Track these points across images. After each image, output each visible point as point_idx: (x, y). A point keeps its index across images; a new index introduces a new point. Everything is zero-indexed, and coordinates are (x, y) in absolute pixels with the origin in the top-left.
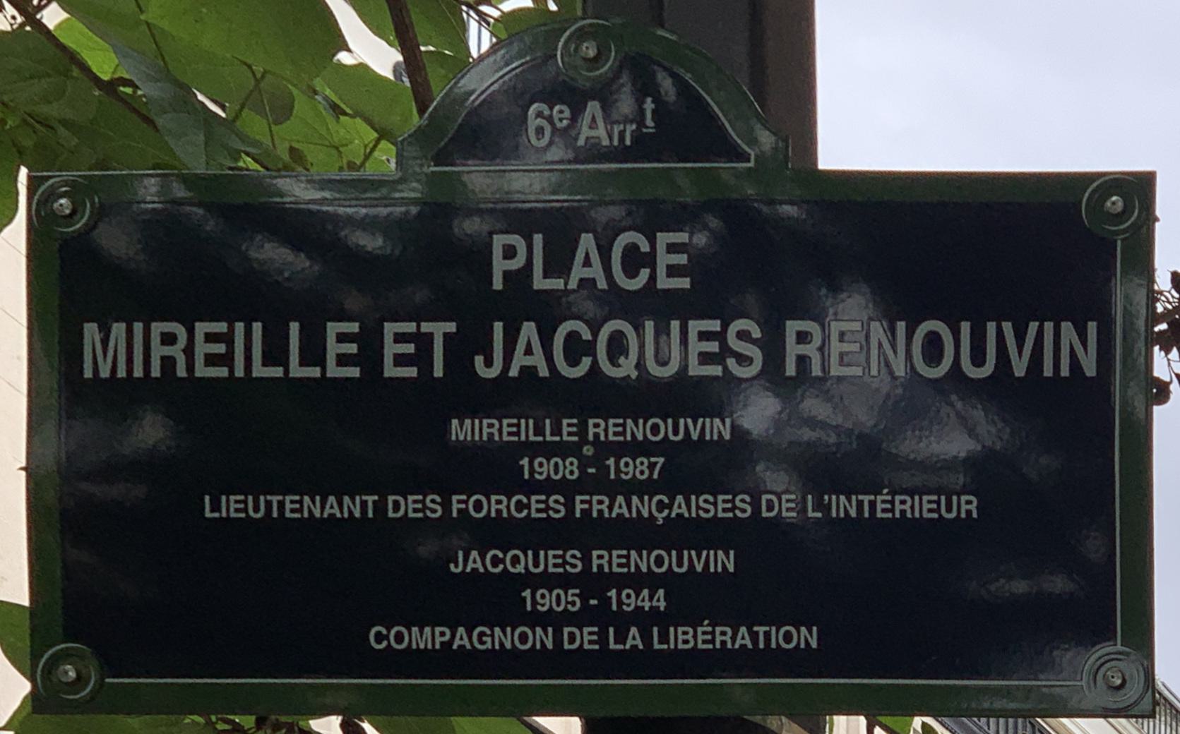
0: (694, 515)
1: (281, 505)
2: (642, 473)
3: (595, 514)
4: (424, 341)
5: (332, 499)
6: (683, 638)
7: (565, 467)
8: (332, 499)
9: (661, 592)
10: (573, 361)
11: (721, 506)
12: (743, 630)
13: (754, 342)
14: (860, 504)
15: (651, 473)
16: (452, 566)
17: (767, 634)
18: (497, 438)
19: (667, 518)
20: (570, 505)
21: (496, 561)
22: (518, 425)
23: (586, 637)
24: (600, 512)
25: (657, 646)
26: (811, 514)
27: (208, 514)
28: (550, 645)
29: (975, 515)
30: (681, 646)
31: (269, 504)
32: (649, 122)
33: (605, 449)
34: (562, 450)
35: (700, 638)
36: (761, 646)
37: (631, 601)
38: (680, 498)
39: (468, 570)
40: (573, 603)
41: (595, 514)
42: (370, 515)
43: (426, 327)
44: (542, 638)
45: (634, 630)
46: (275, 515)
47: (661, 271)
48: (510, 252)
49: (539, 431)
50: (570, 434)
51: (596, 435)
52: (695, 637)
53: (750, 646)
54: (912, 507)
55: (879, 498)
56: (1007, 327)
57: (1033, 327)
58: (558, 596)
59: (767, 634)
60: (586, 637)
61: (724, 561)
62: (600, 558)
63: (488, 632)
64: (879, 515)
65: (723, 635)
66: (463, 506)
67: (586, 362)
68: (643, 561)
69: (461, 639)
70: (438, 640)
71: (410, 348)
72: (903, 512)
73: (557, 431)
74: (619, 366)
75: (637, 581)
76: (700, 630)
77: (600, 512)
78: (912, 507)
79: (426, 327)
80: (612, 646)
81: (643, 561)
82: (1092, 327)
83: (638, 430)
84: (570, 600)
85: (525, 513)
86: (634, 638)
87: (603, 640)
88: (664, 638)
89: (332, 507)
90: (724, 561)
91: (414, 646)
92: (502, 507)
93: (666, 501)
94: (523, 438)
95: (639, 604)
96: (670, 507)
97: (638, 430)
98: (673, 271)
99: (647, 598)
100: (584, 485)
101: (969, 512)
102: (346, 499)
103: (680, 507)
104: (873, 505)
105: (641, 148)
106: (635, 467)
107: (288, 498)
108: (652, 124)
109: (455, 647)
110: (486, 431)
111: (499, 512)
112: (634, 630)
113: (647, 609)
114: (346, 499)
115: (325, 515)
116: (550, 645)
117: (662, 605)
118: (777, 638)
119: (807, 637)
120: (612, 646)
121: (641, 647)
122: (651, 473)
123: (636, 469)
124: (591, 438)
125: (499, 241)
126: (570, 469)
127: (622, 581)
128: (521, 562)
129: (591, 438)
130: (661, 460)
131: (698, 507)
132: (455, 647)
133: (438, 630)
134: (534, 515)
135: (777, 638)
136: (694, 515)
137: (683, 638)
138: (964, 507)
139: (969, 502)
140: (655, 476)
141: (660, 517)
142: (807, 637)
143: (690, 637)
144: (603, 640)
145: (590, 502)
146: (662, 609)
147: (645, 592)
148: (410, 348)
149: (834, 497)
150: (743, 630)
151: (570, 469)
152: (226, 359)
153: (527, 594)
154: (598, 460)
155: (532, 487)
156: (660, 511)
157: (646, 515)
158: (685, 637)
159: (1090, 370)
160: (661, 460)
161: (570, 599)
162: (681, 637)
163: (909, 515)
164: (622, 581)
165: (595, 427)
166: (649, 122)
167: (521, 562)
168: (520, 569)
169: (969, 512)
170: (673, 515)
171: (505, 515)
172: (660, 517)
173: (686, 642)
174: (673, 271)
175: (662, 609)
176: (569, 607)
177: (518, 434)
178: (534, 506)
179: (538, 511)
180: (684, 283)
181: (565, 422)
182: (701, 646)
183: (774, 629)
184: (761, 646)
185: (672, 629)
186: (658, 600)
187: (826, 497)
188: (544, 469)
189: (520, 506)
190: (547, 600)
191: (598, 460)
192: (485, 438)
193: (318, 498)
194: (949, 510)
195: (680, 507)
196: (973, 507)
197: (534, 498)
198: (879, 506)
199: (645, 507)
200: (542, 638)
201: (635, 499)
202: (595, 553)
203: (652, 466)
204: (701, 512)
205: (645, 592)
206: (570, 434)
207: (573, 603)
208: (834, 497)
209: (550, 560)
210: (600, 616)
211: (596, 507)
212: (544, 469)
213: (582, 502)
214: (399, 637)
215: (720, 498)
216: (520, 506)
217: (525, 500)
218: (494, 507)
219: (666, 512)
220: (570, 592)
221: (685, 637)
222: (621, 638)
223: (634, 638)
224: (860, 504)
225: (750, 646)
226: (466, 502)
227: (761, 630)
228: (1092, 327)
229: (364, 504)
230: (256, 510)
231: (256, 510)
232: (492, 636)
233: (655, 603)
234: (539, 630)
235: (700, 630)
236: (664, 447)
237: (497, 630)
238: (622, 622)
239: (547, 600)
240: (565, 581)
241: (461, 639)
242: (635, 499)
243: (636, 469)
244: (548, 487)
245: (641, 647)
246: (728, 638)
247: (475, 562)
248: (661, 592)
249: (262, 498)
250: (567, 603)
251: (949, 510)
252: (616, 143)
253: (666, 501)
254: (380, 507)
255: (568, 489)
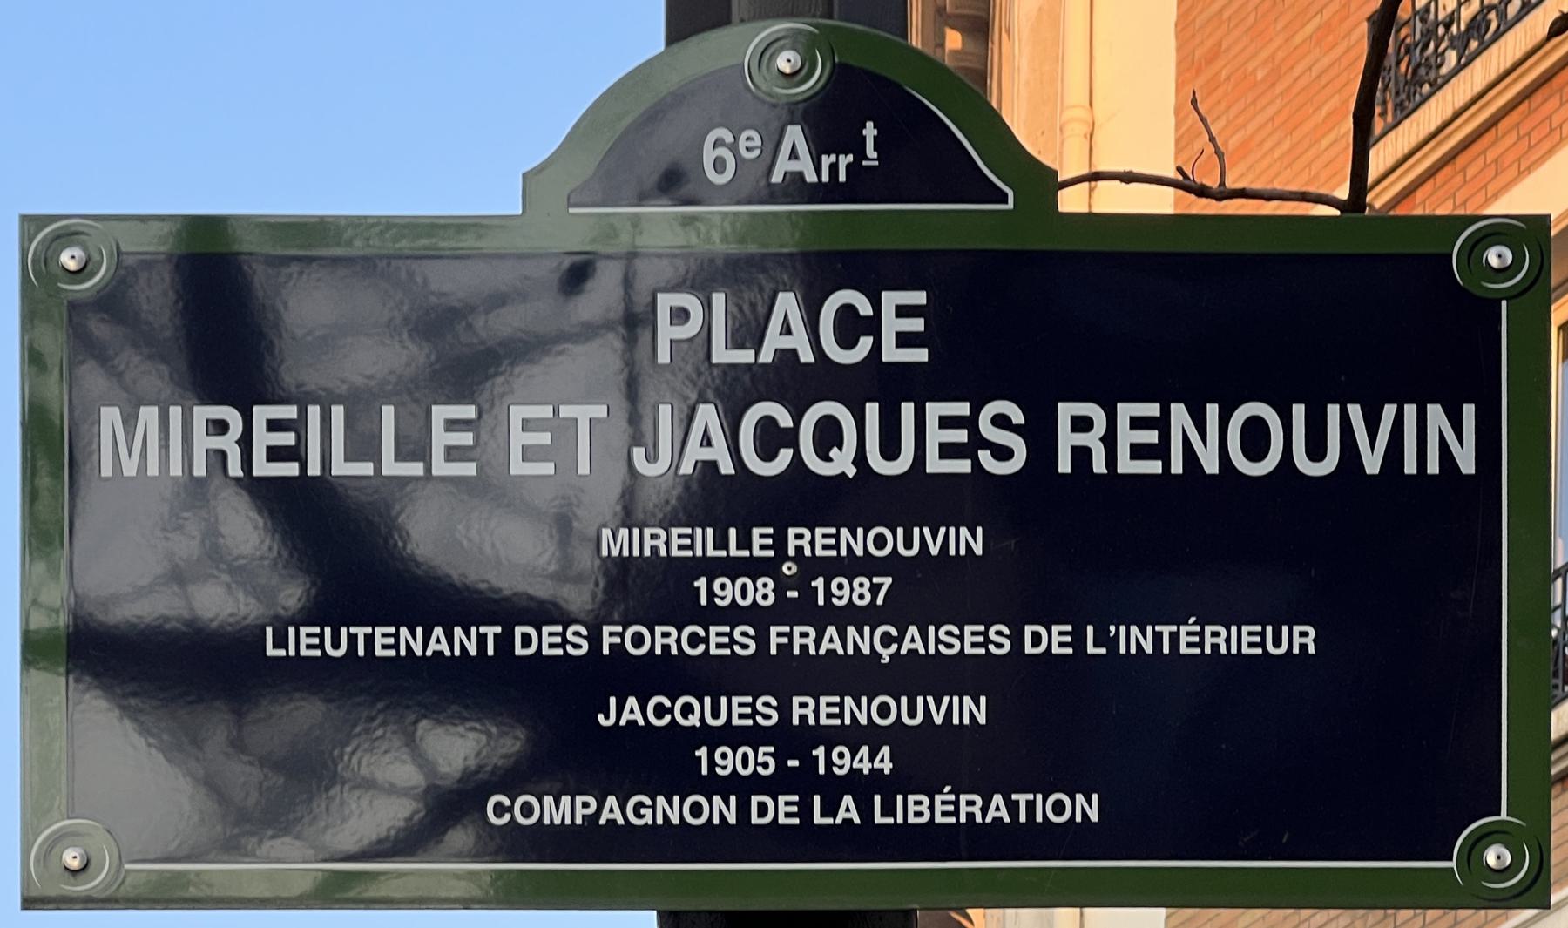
0: (932, 651)
1: (370, 639)
2: (861, 597)
3: (796, 651)
4: (563, 431)
5: (438, 631)
6: (914, 809)
7: (756, 590)
8: (438, 631)
9: (886, 750)
10: (767, 455)
11: (968, 639)
12: (998, 799)
13: (1016, 429)
14: (1158, 637)
15: (874, 597)
16: (601, 717)
17: (1031, 806)
18: (663, 553)
19: (896, 656)
20: (762, 639)
21: (660, 711)
22: (692, 537)
23: (783, 809)
24: (804, 647)
25: (878, 819)
26: (1091, 650)
27: (271, 651)
28: (732, 819)
29: (1312, 650)
30: (912, 820)
31: (352, 639)
32: (871, 152)
33: (811, 566)
34: (754, 568)
35: (939, 808)
36: (1023, 819)
37: (844, 761)
38: (913, 630)
39: (623, 722)
40: (766, 765)
41: (796, 651)
42: (490, 652)
43: (566, 411)
44: (724, 810)
45: (848, 800)
46: (361, 652)
47: (888, 340)
48: (681, 315)
49: (721, 543)
50: (762, 547)
51: (799, 549)
52: (932, 807)
53: (1007, 819)
54: (1228, 640)
55: (1184, 629)
56: (1355, 411)
57: (1389, 411)
58: (745, 756)
59: (1031, 806)
60: (783, 809)
61: (972, 710)
62: (802, 708)
63: (648, 801)
64: (1184, 650)
65: (970, 805)
66: (617, 640)
67: (785, 456)
68: (861, 711)
69: (612, 810)
70: (580, 812)
71: (544, 438)
72: (1215, 647)
73: (745, 542)
74: (829, 460)
75: (854, 736)
76: (938, 798)
77: (804, 647)
78: (1228, 640)
79: (566, 411)
80: (818, 819)
81: (861, 711)
82: (1469, 410)
83: (857, 542)
84: (763, 760)
85: (702, 647)
86: (848, 809)
87: (805, 810)
88: (889, 810)
89: (438, 642)
90: (972, 710)
91: (547, 821)
92: (671, 641)
93: (894, 632)
94: (699, 553)
95: (856, 765)
96: (900, 640)
97: (857, 542)
98: (904, 340)
99: (866, 758)
100: (783, 612)
101: (1303, 647)
102: (458, 631)
103: (912, 640)
104: (1175, 637)
105: (859, 185)
106: (852, 590)
107: (379, 630)
108: (875, 155)
109: (602, 821)
110: (648, 543)
111: (666, 647)
112: (848, 800)
113: (866, 772)
114: (458, 632)
115: (429, 653)
116: (732, 819)
117: (887, 767)
118: (1044, 808)
119: (1085, 807)
120: (818, 819)
121: (857, 821)
122: (874, 597)
123: (854, 591)
124: (792, 552)
125: (665, 302)
126: (763, 592)
127: (830, 738)
128: (693, 712)
129: (792, 552)
130: (888, 581)
131: (938, 641)
132: (602, 821)
133: (579, 799)
134: (713, 651)
135: (1044, 808)
136: (932, 651)
137: (914, 809)
138: (1297, 640)
139: (1304, 634)
140: (880, 601)
141: (886, 654)
142: (1085, 807)
143: (924, 808)
144: (805, 810)
145: (790, 635)
146: (887, 772)
147: (865, 750)
148: (544, 438)
149: (1123, 629)
150: (998, 799)
151: (763, 592)
152: (295, 454)
153: (702, 752)
154: (802, 581)
155: (713, 615)
156: (886, 645)
157: (866, 650)
158: (918, 808)
159: (1467, 463)
160: (888, 581)
161: (761, 759)
162: (912, 808)
163: (1223, 650)
164: (830, 738)
165: (797, 538)
166: (871, 152)
167: (693, 712)
168: (694, 720)
169: (1303, 647)
170: (904, 651)
171: (674, 651)
172: (886, 654)
173: (919, 814)
174: (904, 340)
175: (887, 772)
176: (760, 770)
177: (691, 547)
178: (713, 640)
179: (719, 646)
180: (921, 355)
181: (756, 532)
182: (939, 819)
183: (1039, 797)
184: (1023, 819)
185: (900, 798)
186: (882, 760)
187: (1112, 628)
188: (728, 592)
189: (694, 640)
190: (729, 761)
191: (802, 581)
192: (647, 553)
193: (419, 630)
194: (1277, 643)
195: (912, 640)
196: (1309, 641)
197: (713, 630)
198: (1184, 639)
199: (864, 640)
200: (724, 810)
201: (851, 631)
202: (796, 700)
203: (875, 589)
204: (942, 648)
205: (865, 750)
206: (762, 547)
207: (766, 765)
208: (1123, 629)
209: (735, 710)
210: (802, 782)
211: (797, 641)
212: (728, 592)
213: (779, 635)
214: (527, 810)
215: (968, 629)
216: (694, 640)
217: (702, 633)
218: (659, 641)
219: (894, 647)
220: (762, 750)
221: (918, 808)
222: (830, 809)
223: (848, 809)
224: (1158, 637)
225: (1007, 819)
226: (622, 635)
227: (1022, 798)
228: (1469, 410)
229: (482, 639)
230: (336, 645)
231: (336, 645)
232: (654, 807)
233: (877, 765)
234: (717, 799)
235: (938, 798)
236: (892, 564)
237: (661, 800)
238: (833, 789)
239: (729, 761)
240: (754, 736)
241: (612, 810)
242: (851, 631)
243: (854, 591)
244: (733, 615)
245: (857, 821)
246: (976, 810)
247: (632, 711)
248: (886, 750)
249: (344, 630)
250: (757, 764)
251: (1277, 643)
252: (825, 178)
253: (894, 632)
254: (505, 641)
255: (759, 618)
